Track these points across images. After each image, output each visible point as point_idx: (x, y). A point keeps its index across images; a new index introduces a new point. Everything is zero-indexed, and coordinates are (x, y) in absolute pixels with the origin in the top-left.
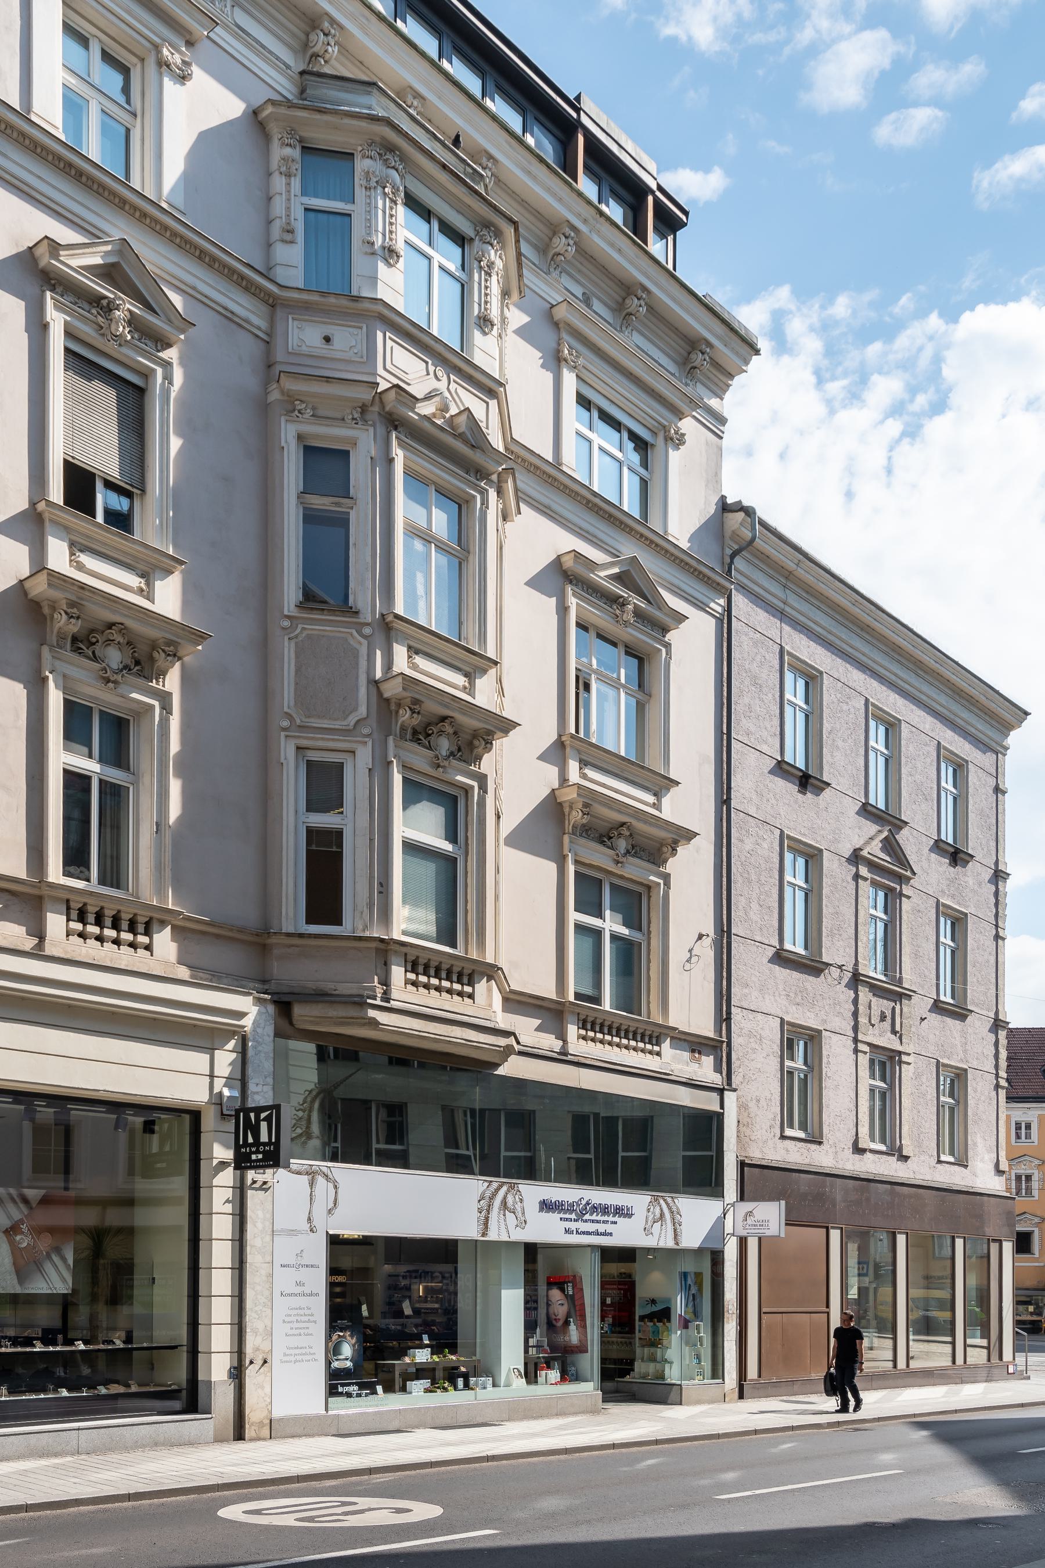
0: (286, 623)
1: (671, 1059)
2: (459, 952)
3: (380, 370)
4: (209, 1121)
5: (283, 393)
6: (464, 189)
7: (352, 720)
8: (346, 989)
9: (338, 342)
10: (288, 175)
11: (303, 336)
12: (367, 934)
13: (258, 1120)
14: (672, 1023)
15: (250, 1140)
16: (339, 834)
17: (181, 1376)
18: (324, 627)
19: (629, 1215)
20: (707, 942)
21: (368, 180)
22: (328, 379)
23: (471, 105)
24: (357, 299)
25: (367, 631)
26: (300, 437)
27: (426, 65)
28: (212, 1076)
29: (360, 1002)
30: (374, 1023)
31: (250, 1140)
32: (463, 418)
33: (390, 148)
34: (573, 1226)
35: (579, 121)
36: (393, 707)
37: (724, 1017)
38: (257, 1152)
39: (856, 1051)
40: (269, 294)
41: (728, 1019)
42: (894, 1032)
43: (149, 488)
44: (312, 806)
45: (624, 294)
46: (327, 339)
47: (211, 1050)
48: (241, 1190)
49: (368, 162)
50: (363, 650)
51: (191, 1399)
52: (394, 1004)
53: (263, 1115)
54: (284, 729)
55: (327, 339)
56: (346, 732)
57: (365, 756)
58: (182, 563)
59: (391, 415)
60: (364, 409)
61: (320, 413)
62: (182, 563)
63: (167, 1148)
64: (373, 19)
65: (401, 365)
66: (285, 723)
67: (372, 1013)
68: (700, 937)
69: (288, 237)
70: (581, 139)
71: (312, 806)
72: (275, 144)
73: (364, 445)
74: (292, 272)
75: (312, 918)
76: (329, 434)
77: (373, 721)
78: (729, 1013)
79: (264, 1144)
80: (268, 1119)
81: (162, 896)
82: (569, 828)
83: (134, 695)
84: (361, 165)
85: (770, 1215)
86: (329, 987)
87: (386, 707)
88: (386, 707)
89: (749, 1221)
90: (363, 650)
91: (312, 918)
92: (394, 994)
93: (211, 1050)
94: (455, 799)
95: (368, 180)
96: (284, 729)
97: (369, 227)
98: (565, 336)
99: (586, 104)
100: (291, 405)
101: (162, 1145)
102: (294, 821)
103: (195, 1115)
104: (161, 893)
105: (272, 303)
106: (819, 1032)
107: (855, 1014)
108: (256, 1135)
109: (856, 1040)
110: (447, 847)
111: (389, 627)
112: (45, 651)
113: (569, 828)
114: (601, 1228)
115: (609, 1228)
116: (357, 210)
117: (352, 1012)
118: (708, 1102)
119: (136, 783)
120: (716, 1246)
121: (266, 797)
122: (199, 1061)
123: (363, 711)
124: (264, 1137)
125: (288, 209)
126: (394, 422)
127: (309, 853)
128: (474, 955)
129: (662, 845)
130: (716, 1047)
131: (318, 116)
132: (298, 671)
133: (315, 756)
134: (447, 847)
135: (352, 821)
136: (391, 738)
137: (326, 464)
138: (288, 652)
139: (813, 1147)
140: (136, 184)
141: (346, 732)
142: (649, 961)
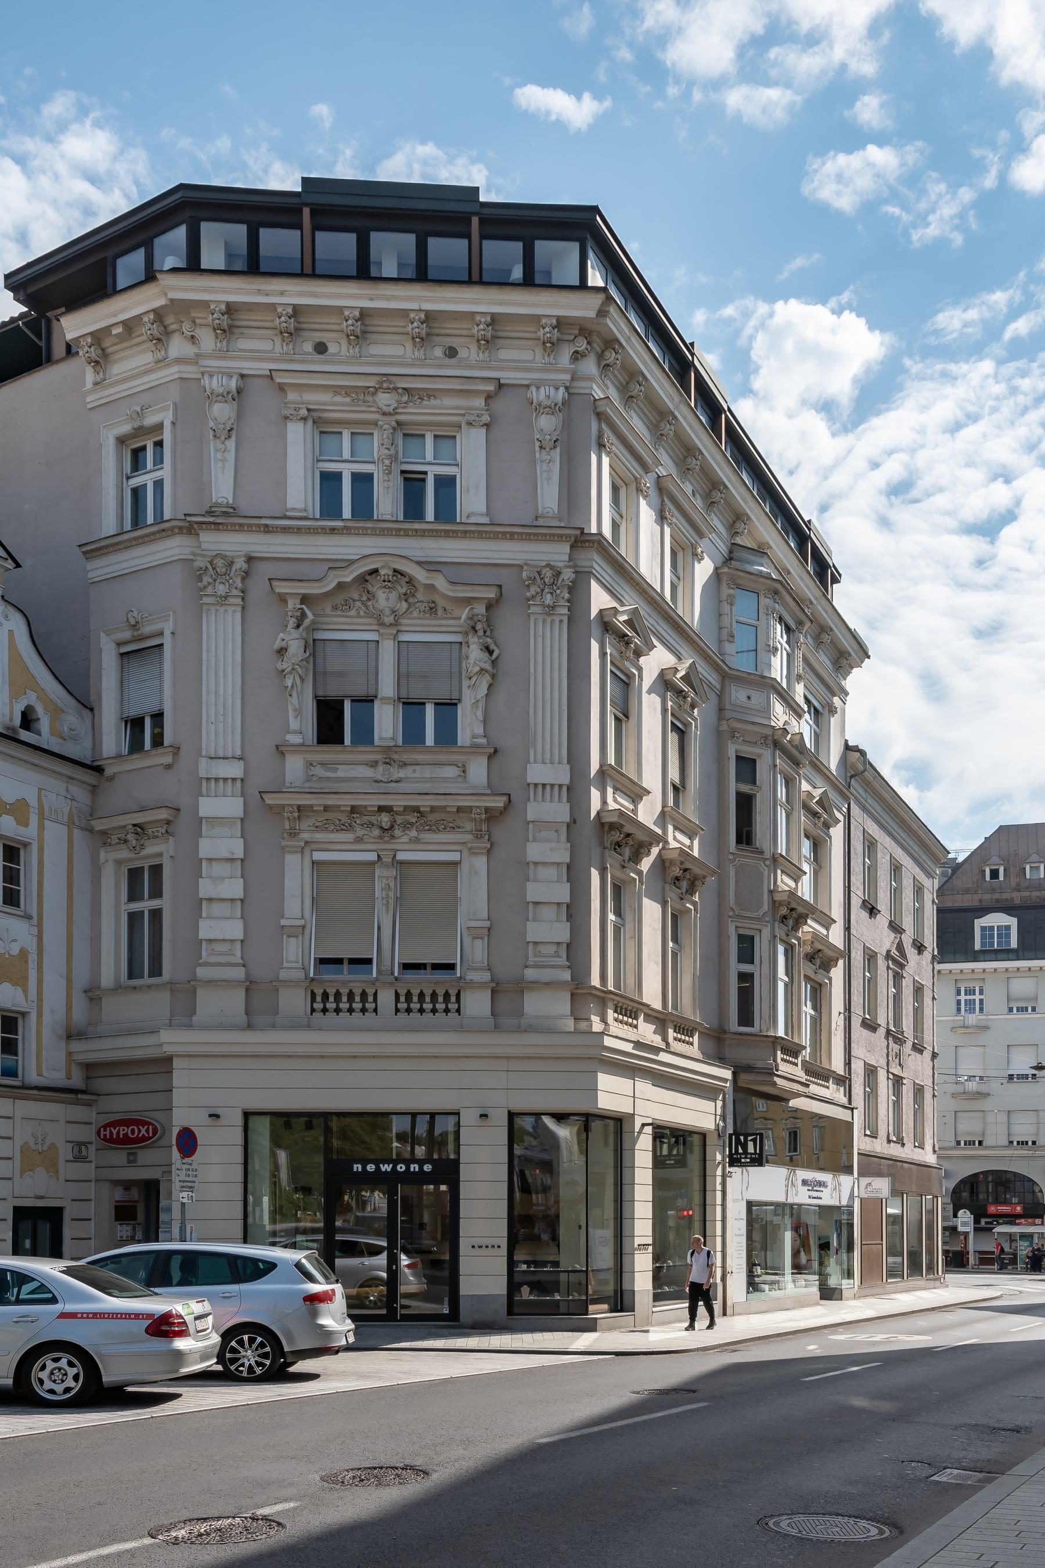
0: (731, 857)
1: (834, 1092)
8: (760, 1064)
9: (753, 700)
11: (738, 695)
16: (752, 975)
18: (747, 859)
22: (753, 723)
24: (764, 677)
25: (768, 863)
30: (775, 1084)
32: (798, 737)
37: (848, 1064)
39: (888, 1078)
40: (724, 671)
41: (849, 1064)
42: (900, 1065)
46: (749, 698)
47: (715, 1100)
48: (724, 1177)
50: (766, 873)
52: (779, 1073)
54: (730, 917)
55: (749, 698)
57: (766, 933)
59: (776, 740)
60: (766, 737)
66: (731, 913)
67: (776, 1079)
73: (765, 759)
75: (741, 1023)
76: (749, 751)
77: (770, 913)
78: (850, 1060)
86: (752, 1063)
87: (775, 904)
88: (775, 904)
90: (766, 873)
91: (741, 1023)
92: (781, 1068)
93: (715, 1100)
96: (730, 917)
97: (768, 637)
100: (733, 733)
103: (703, 1135)
106: (876, 1068)
107: (888, 1055)
108: (745, 1147)
109: (888, 1072)
111: (776, 860)
117: (767, 1078)
122: (708, 1106)
123: (766, 907)
126: (777, 745)
133: (742, 932)
137: (747, 766)
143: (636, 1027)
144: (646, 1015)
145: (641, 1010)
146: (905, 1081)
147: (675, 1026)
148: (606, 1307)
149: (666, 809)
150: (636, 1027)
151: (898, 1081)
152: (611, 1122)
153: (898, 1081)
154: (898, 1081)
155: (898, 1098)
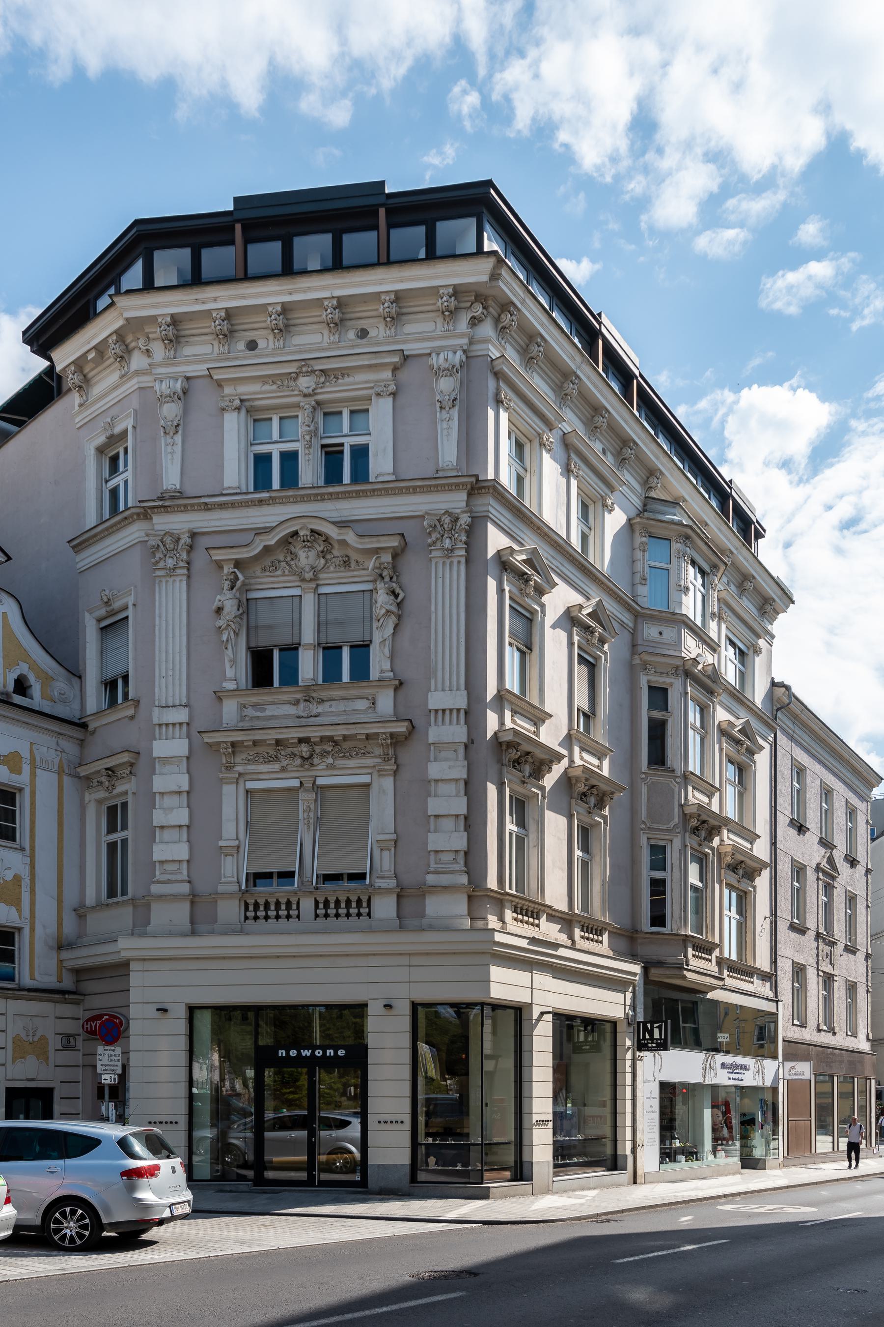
0: (643, 776)
1: (757, 986)
2: (703, 937)
3: (683, 649)
4: (622, 1028)
5: (641, 660)
6: (711, 552)
7: (672, 825)
8: (670, 960)
9: (665, 635)
10: (644, 551)
11: (650, 631)
12: (679, 932)
13: (652, 1027)
14: (757, 966)
15: (647, 1037)
16: (664, 881)
17: (609, 1151)
18: (659, 777)
19: (748, 1070)
20: (768, 921)
21: (679, 554)
22: (664, 655)
23: (704, 502)
24: (674, 614)
25: (678, 780)
26: (648, 682)
27: (691, 486)
28: (625, 1005)
29: (680, 967)
30: (685, 977)
31: (647, 1037)
32: (711, 667)
33: (687, 537)
34: (731, 1075)
35: (600, 330)
36: (688, 818)
37: (774, 962)
38: (652, 1043)
39: (818, 975)
40: (636, 611)
41: (776, 962)
42: (831, 964)
43: (598, 714)
44: (653, 868)
45: (622, 445)
46: (661, 633)
47: (624, 992)
48: (634, 1060)
49: (679, 545)
50: (677, 790)
51: (614, 1164)
52: (690, 967)
53: (655, 1025)
54: (642, 829)
55: (661, 633)
56: (669, 831)
57: (677, 843)
58: (612, 751)
59: (686, 670)
60: (677, 668)
61: (658, 670)
62: (612, 751)
63: (590, 1039)
64: (676, 469)
65: (691, 647)
66: (643, 826)
67: (685, 972)
68: (766, 918)
69: (643, 582)
70: (600, 342)
71: (653, 868)
72: (637, 534)
73: (676, 687)
74: (645, 599)
75: (653, 924)
76: (660, 681)
77: (681, 825)
78: (776, 959)
79: (657, 1039)
80: (660, 1028)
81: (604, 916)
82: (724, 866)
83: (533, 789)
84: (676, 546)
85: (805, 1070)
86: (663, 959)
87: (686, 817)
88: (686, 818)
89: (793, 1072)
90: (677, 790)
91: (653, 924)
92: (691, 963)
93: (624, 992)
94: (701, 859)
95: (679, 554)
96: (642, 829)
97: (679, 578)
98: (572, 455)
99: (604, 319)
100: (645, 666)
101: (586, 1037)
102: (646, 874)
103: (614, 1023)
104: (604, 916)
105: (637, 615)
106: (805, 966)
107: (818, 955)
108: (651, 1033)
109: (818, 970)
110: (700, 884)
111: (687, 777)
112: (573, 801)
113: (724, 866)
114: (740, 1076)
115: (740, 1076)
116: (673, 568)
117: (676, 972)
118: (769, 1007)
119: (591, 860)
120: (775, 1085)
121: (634, 862)
122: (618, 997)
123: (676, 820)
124: (657, 1035)
125: (644, 568)
126: (688, 674)
127: (651, 890)
128: (710, 939)
129: (754, 871)
130: (770, 977)
131: (660, 524)
132: (648, 800)
133: (653, 842)
134: (700, 884)
135: (670, 876)
136: (687, 834)
137: (659, 696)
138: (644, 790)
139: (803, 1029)
140: (591, 560)
141: (669, 831)
142: (746, 932)
143: (538, 926)
144: (548, 915)
145: (544, 911)
146: (836, 978)
147: (583, 926)
148: (508, 1174)
149: (572, 732)
150: (538, 926)
151: (829, 979)
152: (512, 1011)
153: (829, 978)
154: (829, 979)
155: (829, 993)
